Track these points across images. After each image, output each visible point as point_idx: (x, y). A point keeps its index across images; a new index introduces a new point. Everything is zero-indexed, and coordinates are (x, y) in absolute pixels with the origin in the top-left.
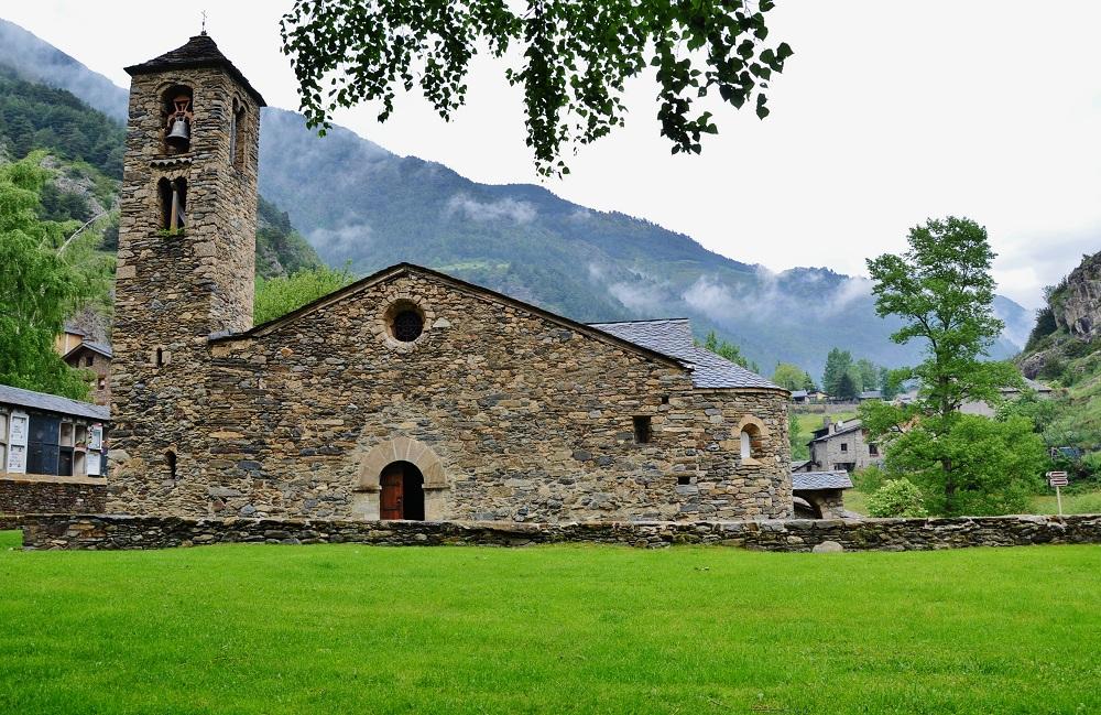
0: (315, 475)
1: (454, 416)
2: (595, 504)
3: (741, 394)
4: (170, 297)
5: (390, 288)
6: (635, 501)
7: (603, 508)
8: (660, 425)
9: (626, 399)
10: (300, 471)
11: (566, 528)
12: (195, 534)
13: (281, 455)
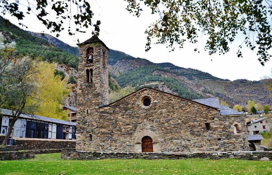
0: (126, 140)
1: (160, 124)
2: (196, 146)
3: (233, 116)
4: (90, 97)
5: (142, 93)
6: (207, 145)
7: (199, 147)
8: (212, 125)
9: (203, 119)
10: (122, 139)
11: (193, 154)
12: (101, 156)
13: (117, 135)
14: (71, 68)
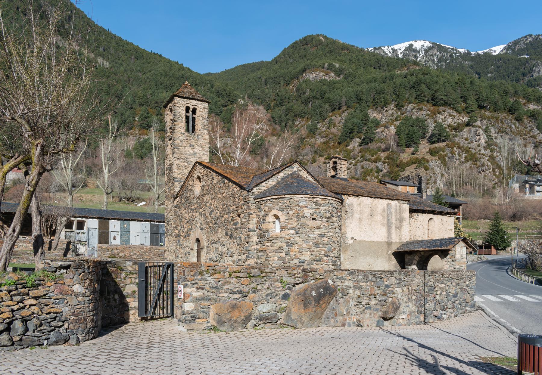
14: (441, 109)
